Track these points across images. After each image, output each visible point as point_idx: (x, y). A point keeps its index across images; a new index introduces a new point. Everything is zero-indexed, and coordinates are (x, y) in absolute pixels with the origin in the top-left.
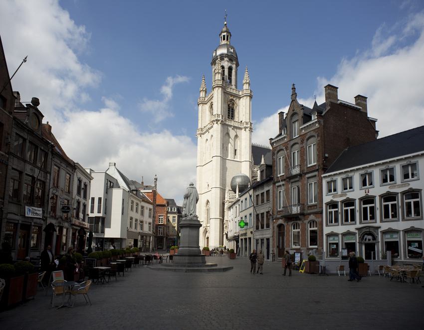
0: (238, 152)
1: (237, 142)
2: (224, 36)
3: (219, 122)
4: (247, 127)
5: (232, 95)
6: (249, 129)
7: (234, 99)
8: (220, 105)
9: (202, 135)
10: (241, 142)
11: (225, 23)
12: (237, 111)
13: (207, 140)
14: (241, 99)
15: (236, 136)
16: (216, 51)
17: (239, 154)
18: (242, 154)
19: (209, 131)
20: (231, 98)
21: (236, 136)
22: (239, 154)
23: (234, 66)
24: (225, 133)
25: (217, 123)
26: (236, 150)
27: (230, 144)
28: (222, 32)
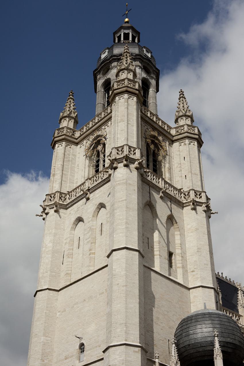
0: (177, 259)
1: (173, 235)
2: (126, 36)
3: (133, 166)
4: (200, 204)
5: (154, 129)
6: (204, 207)
7: (160, 138)
8: (135, 128)
9: (61, 211)
10: (182, 235)
11: (127, 20)
12: (167, 165)
13: (80, 220)
14: (176, 144)
15: (171, 219)
16: (111, 49)
17: (179, 265)
18: (190, 267)
19: (91, 196)
20: (152, 133)
21: (171, 219)
22: (179, 265)
23: (153, 82)
24: (145, 201)
25: (126, 166)
26: (170, 254)
27: (156, 235)
28: (122, 28)
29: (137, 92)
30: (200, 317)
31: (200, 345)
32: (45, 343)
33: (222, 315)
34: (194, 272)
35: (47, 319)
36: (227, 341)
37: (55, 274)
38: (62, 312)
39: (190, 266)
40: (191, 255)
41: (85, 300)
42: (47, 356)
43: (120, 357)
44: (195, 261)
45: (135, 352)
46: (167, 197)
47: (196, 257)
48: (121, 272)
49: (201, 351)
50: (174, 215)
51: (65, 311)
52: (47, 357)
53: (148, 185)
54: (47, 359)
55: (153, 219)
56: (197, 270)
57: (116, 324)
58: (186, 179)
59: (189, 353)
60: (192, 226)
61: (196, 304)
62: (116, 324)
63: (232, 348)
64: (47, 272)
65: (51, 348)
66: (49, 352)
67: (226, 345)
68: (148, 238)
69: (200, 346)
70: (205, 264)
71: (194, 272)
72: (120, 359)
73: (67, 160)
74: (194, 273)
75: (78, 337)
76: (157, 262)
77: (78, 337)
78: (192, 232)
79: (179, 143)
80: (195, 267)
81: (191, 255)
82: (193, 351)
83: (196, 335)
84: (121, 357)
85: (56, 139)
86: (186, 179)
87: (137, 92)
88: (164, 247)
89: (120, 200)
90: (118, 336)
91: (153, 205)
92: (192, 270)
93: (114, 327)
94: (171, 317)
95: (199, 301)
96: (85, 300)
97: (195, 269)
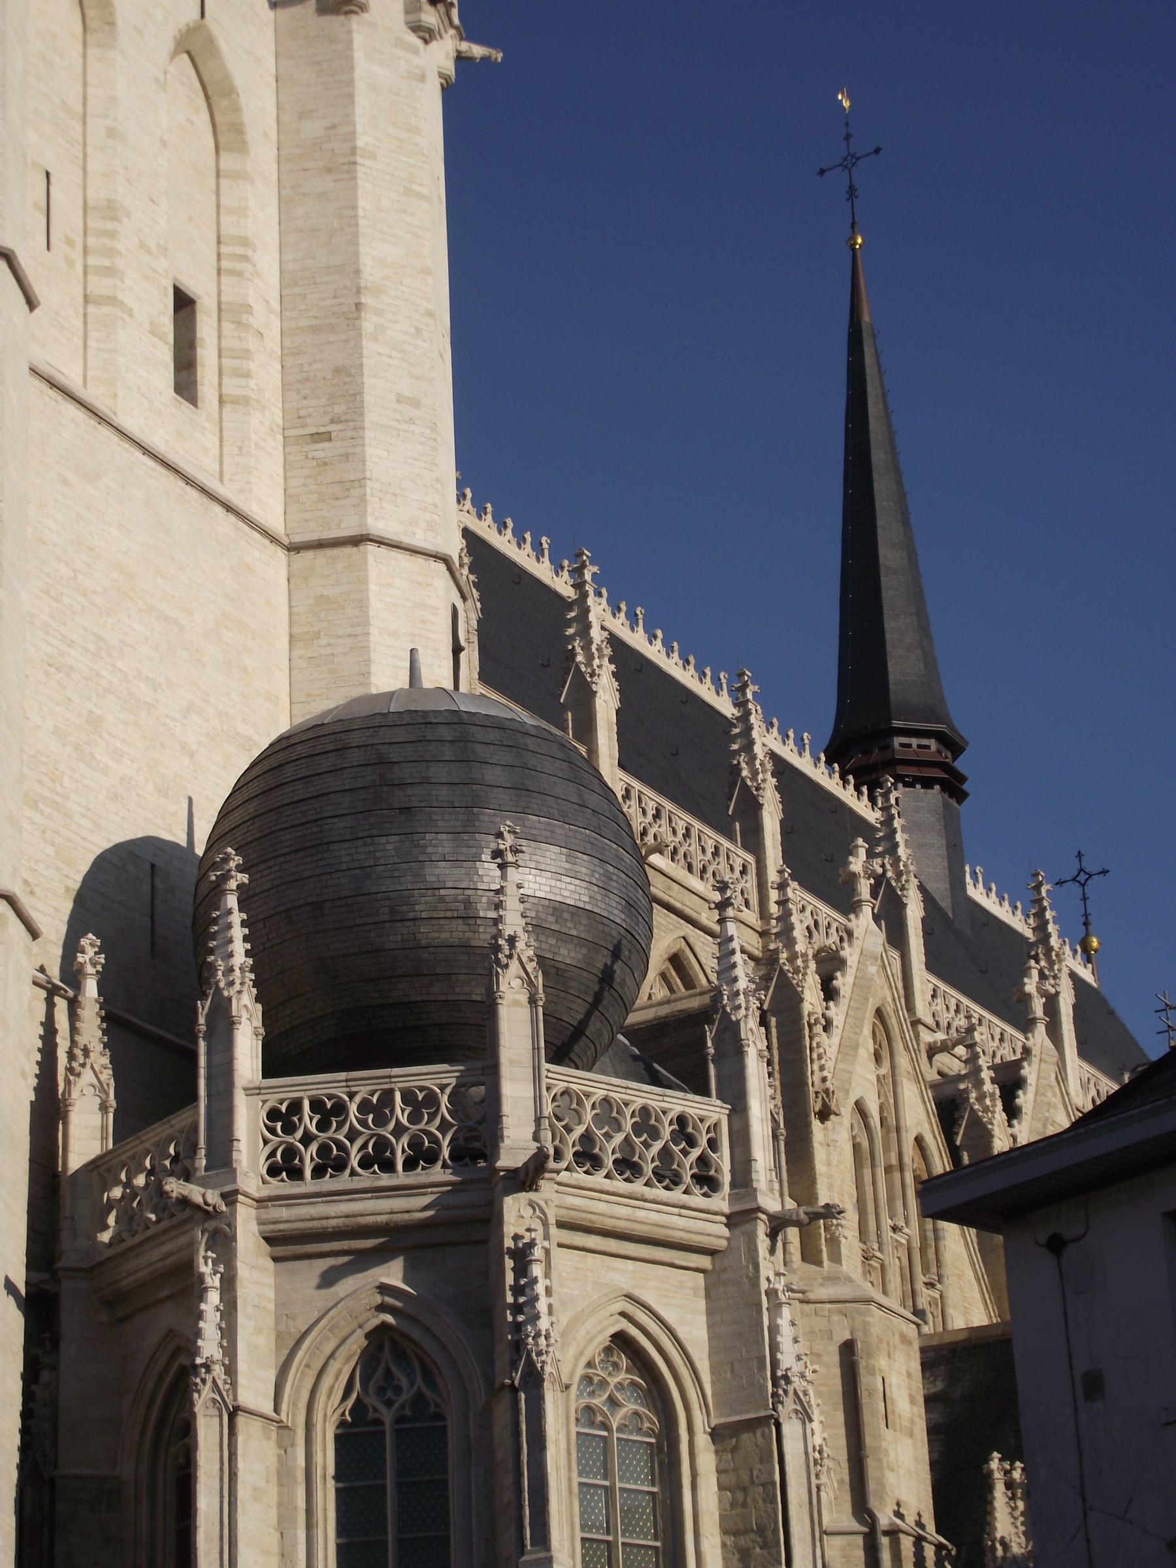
30: (400, 735)
31: (386, 910)
33: (533, 732)
34: (326, 445)
36: (559, 898)
39: (305, 403)
40: (314, 329)
44: (338, 371)
47: (347, 341)
49: (392, 946)
50: (215, 30)
56: (350, 434)
60: (333, 127)
61: (329, 651)
63: (581, 941)
67: (551, 919)
68: (48, 174)
69: (386, 918)
71: (330, 439)
74: (322, 450)
76: (99, 350)
78: (329, 170)
80: (339, 409)
81: (314, 329)
88: (150, 252)
92: (313, 430)
94: (173, 719)
95: (349, 631)
97: (332, 421)
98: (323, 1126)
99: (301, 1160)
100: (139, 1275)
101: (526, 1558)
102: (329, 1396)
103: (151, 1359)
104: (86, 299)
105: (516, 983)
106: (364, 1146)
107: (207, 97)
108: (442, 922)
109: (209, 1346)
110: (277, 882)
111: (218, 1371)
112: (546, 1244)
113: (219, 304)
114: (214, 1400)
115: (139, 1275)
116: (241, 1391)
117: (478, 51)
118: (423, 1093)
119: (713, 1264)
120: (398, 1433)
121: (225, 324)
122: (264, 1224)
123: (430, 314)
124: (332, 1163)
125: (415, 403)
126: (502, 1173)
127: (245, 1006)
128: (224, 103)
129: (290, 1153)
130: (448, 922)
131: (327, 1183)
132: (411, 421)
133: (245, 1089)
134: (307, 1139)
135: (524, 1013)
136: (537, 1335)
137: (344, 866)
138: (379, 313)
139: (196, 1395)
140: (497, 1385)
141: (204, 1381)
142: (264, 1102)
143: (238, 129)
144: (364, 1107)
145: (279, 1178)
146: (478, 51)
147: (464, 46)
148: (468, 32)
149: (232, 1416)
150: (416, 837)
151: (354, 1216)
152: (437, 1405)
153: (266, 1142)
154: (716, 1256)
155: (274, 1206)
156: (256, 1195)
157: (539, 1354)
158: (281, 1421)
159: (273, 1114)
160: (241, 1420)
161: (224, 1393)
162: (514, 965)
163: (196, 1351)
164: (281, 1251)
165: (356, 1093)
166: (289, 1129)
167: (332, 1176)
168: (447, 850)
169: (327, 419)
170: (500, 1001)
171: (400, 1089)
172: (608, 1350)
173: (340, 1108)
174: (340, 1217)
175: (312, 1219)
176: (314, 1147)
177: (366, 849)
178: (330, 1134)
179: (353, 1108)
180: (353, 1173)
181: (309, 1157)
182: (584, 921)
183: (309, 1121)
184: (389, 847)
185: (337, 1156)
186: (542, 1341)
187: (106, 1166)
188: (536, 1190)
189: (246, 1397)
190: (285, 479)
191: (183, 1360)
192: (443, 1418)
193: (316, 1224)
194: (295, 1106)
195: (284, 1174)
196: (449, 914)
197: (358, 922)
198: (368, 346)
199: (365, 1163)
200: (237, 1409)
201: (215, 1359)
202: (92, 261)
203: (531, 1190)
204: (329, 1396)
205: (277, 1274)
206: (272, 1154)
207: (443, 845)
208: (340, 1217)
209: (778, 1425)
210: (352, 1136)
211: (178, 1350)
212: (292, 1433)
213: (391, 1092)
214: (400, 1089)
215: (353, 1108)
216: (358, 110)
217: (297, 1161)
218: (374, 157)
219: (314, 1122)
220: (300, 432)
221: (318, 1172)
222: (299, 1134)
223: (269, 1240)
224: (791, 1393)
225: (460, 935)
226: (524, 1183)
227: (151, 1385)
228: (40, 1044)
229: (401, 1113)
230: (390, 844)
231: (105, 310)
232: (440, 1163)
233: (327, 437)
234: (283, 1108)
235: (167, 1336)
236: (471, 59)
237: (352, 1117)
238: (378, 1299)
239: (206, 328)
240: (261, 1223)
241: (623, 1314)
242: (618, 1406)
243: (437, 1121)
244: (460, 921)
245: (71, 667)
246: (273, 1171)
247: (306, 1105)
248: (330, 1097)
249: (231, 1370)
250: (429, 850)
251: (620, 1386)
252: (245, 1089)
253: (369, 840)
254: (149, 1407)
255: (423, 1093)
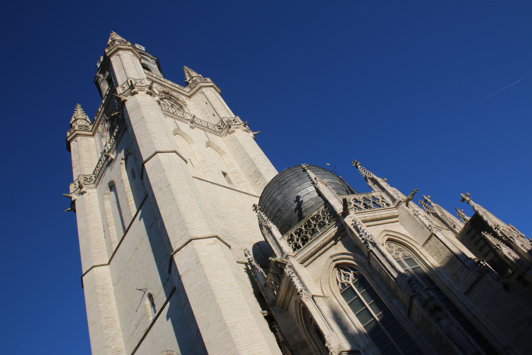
29: (131, 48)
32: (107, 325)
35: (102, 299)
37: (98, 250)
38: (118, 282)
40: (249, 169)
41: (137, 249)
42: (114, 340)
43: (191, 258)
44: (255, 171)
45: (208, 244)
46: (198, 128)
48: (159, 176)
51: (120, 278)
52: (114, 341)
53: (172, 117)
54: (115, 343)
55: (190, 145)
57: (172, 228)
58: (214, 116)
59: (285, 220)
62: (172, 228)
64: (89, 252)
65: (116, 329)
66: (115, 335)
68: (190, 159)
70: (266, 170)
72: (192, 260)
73: (85, 150)
74: (258, 183)
75: (140, 290)
77: (140, 290)
79: (197, 95)
80: (257, 176)
81: (249, 169)
82: (288, 215)
83: (283, 193)
84: (193, 257)
85: (68, 139)
86: (214, 116)
87: (131, 48)
89: (137, 121)
90: (179, 238)
91: (185, 133)
93: (172, 232)
96: (137, 249)
97: (257, 178)
98: (299, 235)
99: (299, 244)
100: (283, 295)
101: (398, 281)
102: (334, 286)
103: (296, 310)
104: (204, 173)
105: (321, 185)
106: (310, 233)
107: (216, 151)
108: (304, 197)
109: (299, 287)
110: (271, 212)
111: (304, 291)
112: (358, 221)
113: (231, 172)
114: (307, 297)
115: (283, 295)
116: (311, 293)
117: (256, 133)
118: (316, 216)
119: (399, 219)
120: (354, 284)
121: (233, 174)
122: (298, 260)
123: (265, 159)
124: (305, 241)
125: (270, 170)
126: (340, 215)
127: (271, 226)
128: (219, 150)
129: (296, 244)
130: (305, 196)
131: (306, 244)
132: (270, 172)
133: (280, 239)
134: (298, 240)
135: (326, 188)
136: (369, 236)
137: (280, 200)
138: (257, 162)
139: (302, 298)
140: (366, 254)
141: (302, 295)
142: (285, 239)
143: (223, 152)
144: (305, 227)
145: (296, 250)
146: (256, 133)
147: (254, 133)
148: (253, 131)
149: (313, 298)
150: (290, 186)
151: (316, 246)
152: (359, 273)
153: (290, 246)
154: (398, 217)
155: (298, 255)
156: (294, 255)
157: (371, 239)
158: (326, 296)
159: (288, 240)
160: (315, 298)
161: (308, 294)
162: (319, 182)
163: (297, 289)
164: (306, 264)
165: (302, 225)
166: (293, 240)
167: (307, 243)
168: (297, 184)
169: (257, 178)
170: (319, 189)
171: (310, 218)
172: (388, 245)
173: (301, 230)
174: (313, 249)
175: (307, 253)
176: (300, 240)
177: (282, 194)
178: (302, 235)
179: (303, 228)
180: (311, 239)
181: (300, 243)
182: (332, 185)
183: (296, 237)
184: (286, 190)
185: (306, 239)
186: (370, 237)
187: (267, 283)
188: (350, 214)
189: (313, 294)
190: (255, 190)
191: (302, 305)
192: (362, 275)
193: (309, 253)
194: (292, 236)
195: (297, 249)
196: (305, 195)
197: (289, 207)
198: (257, 166)
199: (312, 235)
200: (313, 297)
201: (302, 288)
202: (201, 166)
203: (348, 215)
204: (334, 286)
205: (307, 270)
206: (292, 247)
207: (297, 184)
208: (313, 249)
209: (435, 235)
210: (306, 233)
211: (300, 304)
212: (330, 298)
213: (309, 220)
214: (310, 218)
215: (303, 228)
216: (240, 141)
217: (298, 245)
218: (245, 145)
219: (297, 236)
220: (253, 183)
221: (303, 244)
222: (295, 240)
223: (302, 263)
224: (433, 228)
225: (309, 197)
226: (346, 213)
227: (299, 316)
228: (249, 279)
229: (313, 222)
230: (286, 190)
231: (208, 172)
232: (327, 225)
233: (258, 180)
234: (290, 238)
235: (296, 302)
236: (256, 134)
237: (304, 230)
238: (332, 260)
239: (229, 175)
240: (297, 260)
241: (387, 235)
242: (399, 254)
243: (322, 219)
244: (308, 195)
245: (223, 216)
246: (294, 250)
247: (294, 234)
248: (297, 229)
249: (306, 290)
250: (294, 186)
251: (396, 250)
252: (280, 239)
253: (282, 192)
254: (302, 321)
255: (316, 216)
